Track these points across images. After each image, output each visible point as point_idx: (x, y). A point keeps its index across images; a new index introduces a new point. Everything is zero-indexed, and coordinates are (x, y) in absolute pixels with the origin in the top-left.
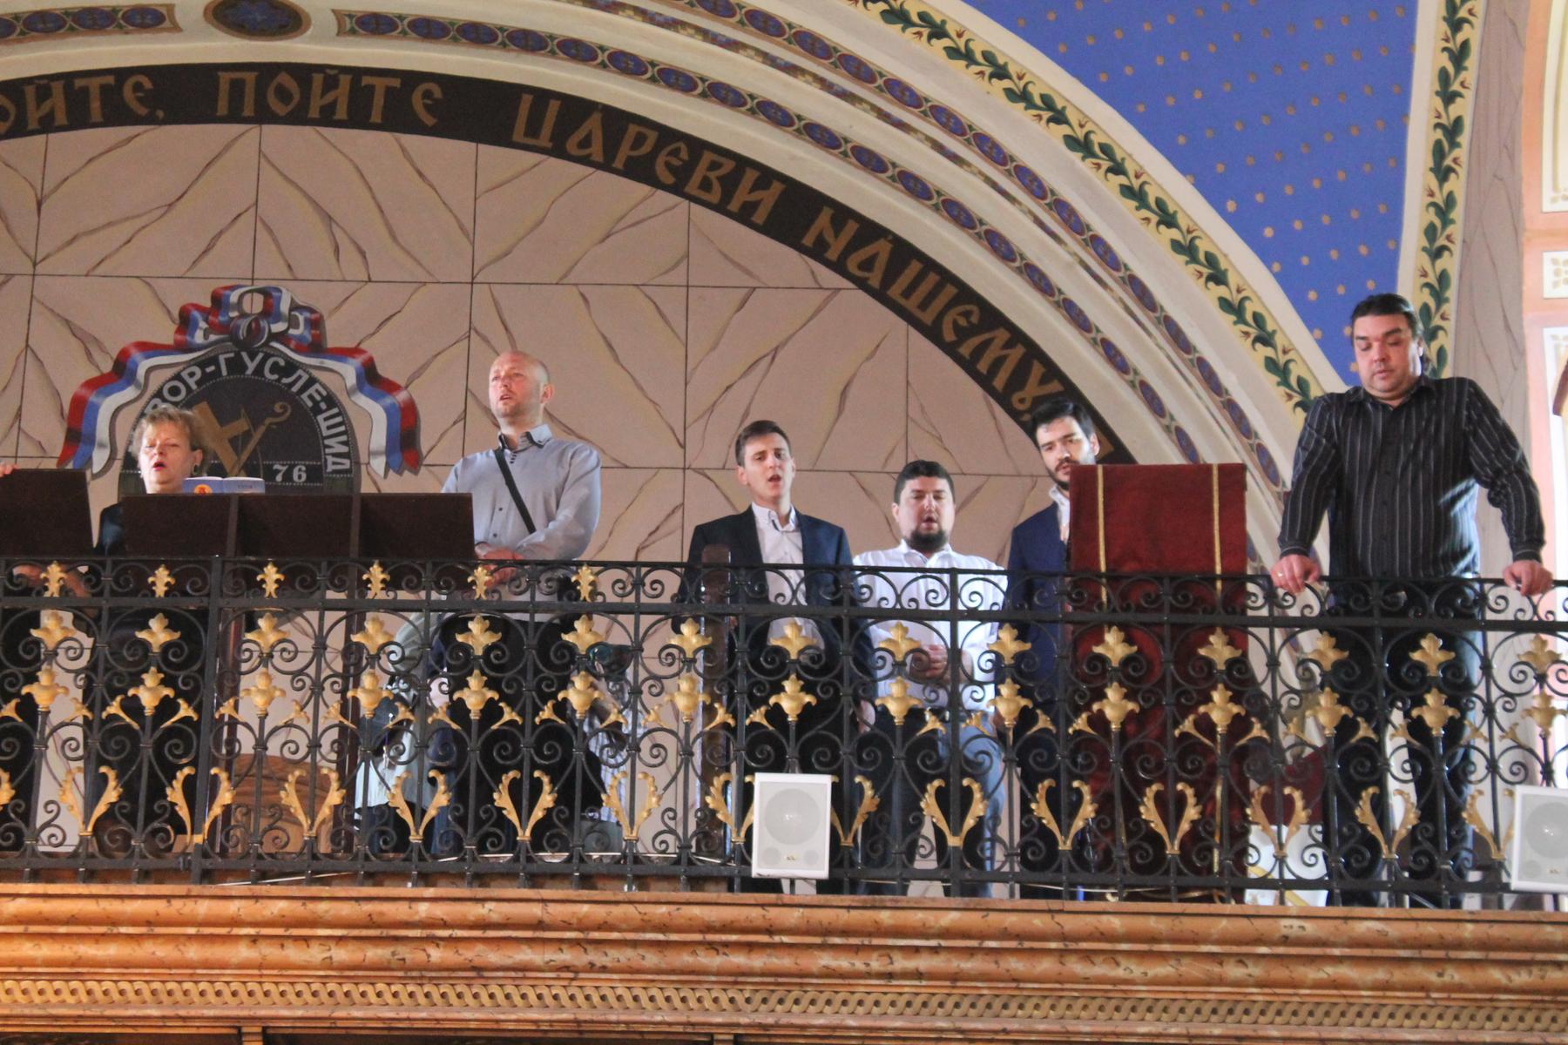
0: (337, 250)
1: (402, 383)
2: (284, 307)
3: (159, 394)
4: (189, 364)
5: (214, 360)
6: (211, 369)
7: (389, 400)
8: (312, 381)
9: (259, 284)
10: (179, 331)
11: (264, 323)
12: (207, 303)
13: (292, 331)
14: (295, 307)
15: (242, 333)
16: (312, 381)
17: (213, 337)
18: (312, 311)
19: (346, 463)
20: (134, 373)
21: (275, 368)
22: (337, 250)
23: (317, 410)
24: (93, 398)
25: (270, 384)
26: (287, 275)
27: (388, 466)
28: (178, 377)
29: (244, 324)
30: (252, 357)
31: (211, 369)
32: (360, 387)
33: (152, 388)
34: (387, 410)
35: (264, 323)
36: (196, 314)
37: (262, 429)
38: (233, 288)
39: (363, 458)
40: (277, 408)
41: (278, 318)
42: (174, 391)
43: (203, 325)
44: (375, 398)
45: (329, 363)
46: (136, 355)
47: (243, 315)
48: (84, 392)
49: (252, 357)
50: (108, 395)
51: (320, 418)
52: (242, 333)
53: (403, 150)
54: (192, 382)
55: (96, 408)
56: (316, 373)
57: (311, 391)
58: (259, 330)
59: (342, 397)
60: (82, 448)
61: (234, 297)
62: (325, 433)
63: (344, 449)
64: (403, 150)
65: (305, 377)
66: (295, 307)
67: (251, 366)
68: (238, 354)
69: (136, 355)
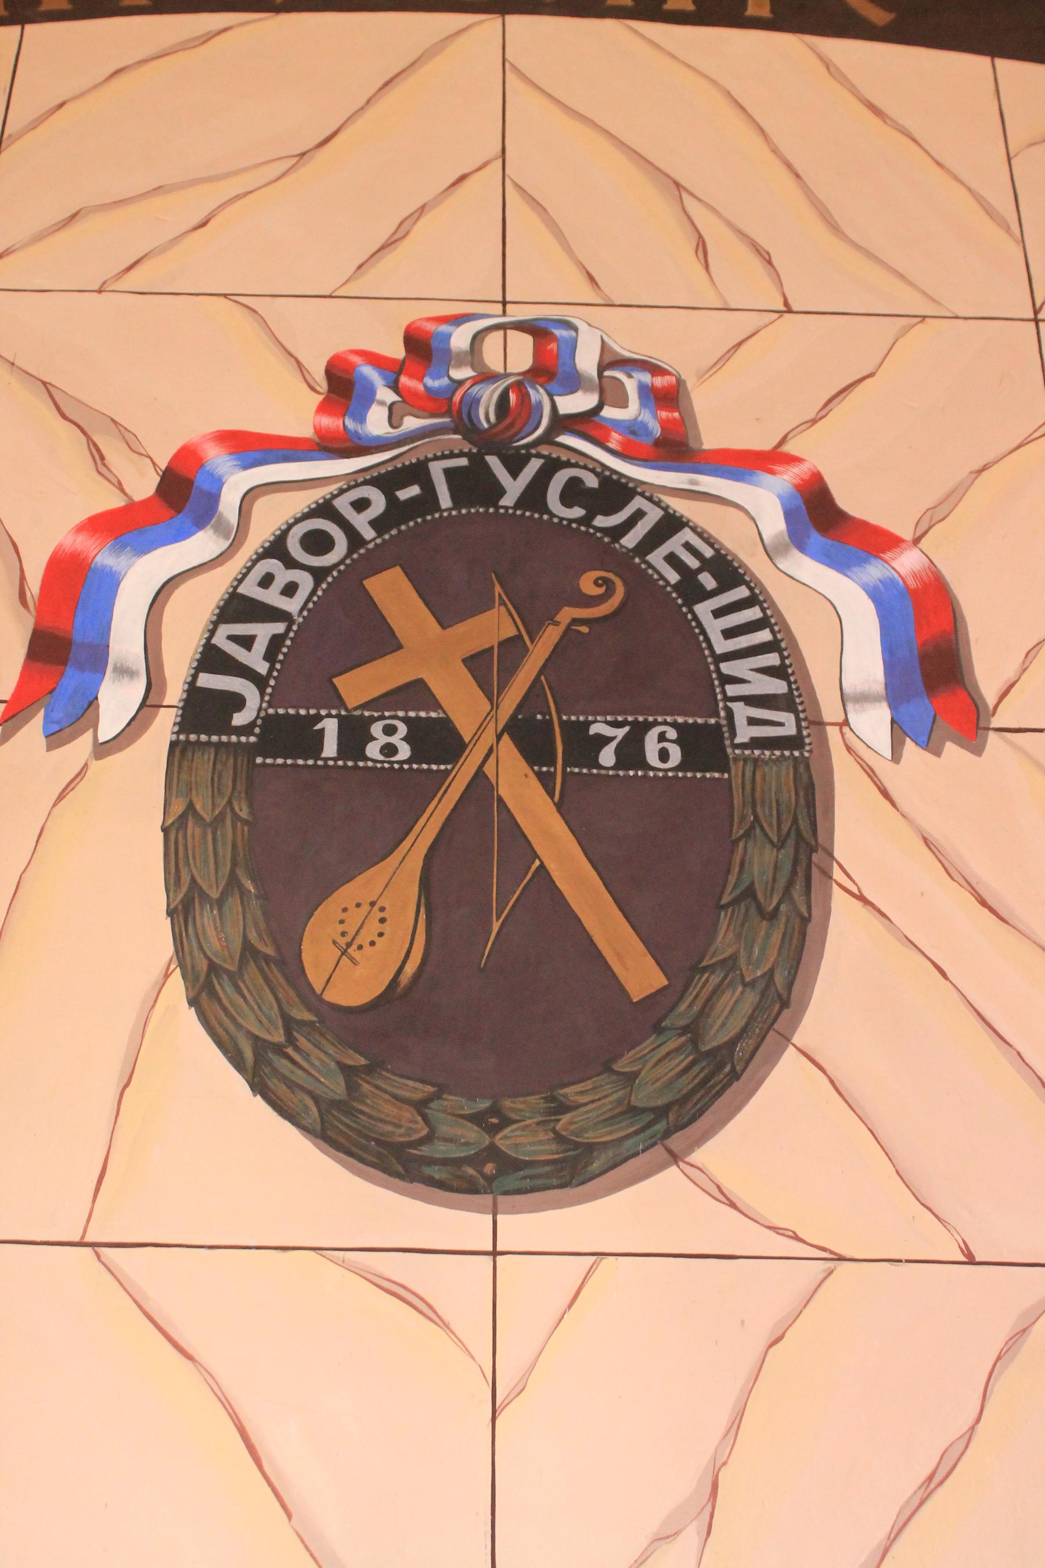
0: (701, 247)
1: (906, 533)
2: (587, 361)
3: (276, 549)
4: (353, 481)
5: (418, 473)
6: (409, 492)
7: (875, 571)
8: (671, 524)
9: (516, 313)
10: (323, 408)
11: (538, 395)
12: (397, 351)
13: (609, 412)
14: (610, 361)
15: (486, 413)
16: (671, 524)
17: (411, 423)
18: (656, 370)
19: (787, 725)
20: (213, 498)
21: (573, 493)
22: (701, 247)
23: (694, 594)
24: (105, 558)
25: (564, 527)
26: (588, 295)
27: (899, 730)
28: (325, 510)
29: (488, 396)
30: (514, 469)
31: (409, 492)
32: (797, 539)
33: (260, 534)
34: (878, 595)
35: (538, 395)
36: (368, 371)
37: (551, 636)
38: (458, 320)
39: (830, 710)
40: (587, 584)
41: (574, 383)
42: (317, 543)
43: (385, 395)
44: (841, 565)
45: (709, 483)
46: (218, 459)
47: (486, 377)
48: (83, 543)
49: (514, 469)
50: (143, 550)
51: (703, 610)
52: (486, 413)
53: (828, 65)
54: (361, 522)
55: (112, 582)
56: (680, 506)
57: (674, 544)
58: (529, 411)
59: (755, 563)
60: (71, 678)
61: (460, 339)
62: (721, 646)
63: (777, 687)
64: (828, 65)
65: (654, 515)
66: (610, 361)
67: (513, 488)
68: (478, 462)
69: (218, 459)
